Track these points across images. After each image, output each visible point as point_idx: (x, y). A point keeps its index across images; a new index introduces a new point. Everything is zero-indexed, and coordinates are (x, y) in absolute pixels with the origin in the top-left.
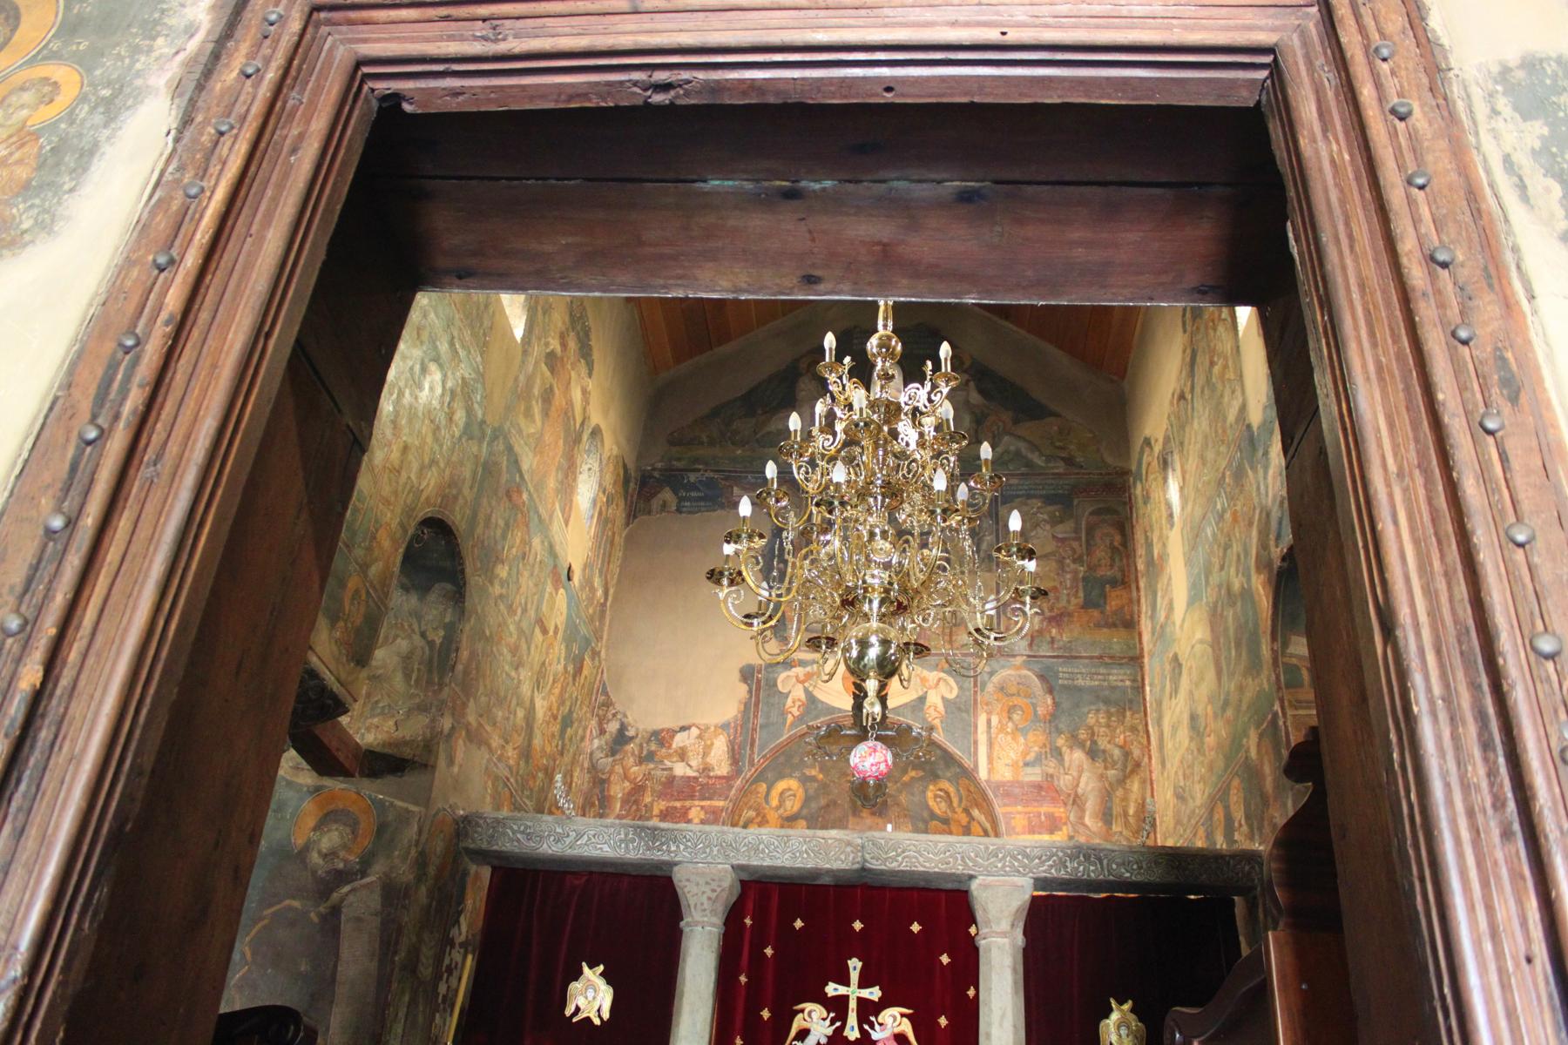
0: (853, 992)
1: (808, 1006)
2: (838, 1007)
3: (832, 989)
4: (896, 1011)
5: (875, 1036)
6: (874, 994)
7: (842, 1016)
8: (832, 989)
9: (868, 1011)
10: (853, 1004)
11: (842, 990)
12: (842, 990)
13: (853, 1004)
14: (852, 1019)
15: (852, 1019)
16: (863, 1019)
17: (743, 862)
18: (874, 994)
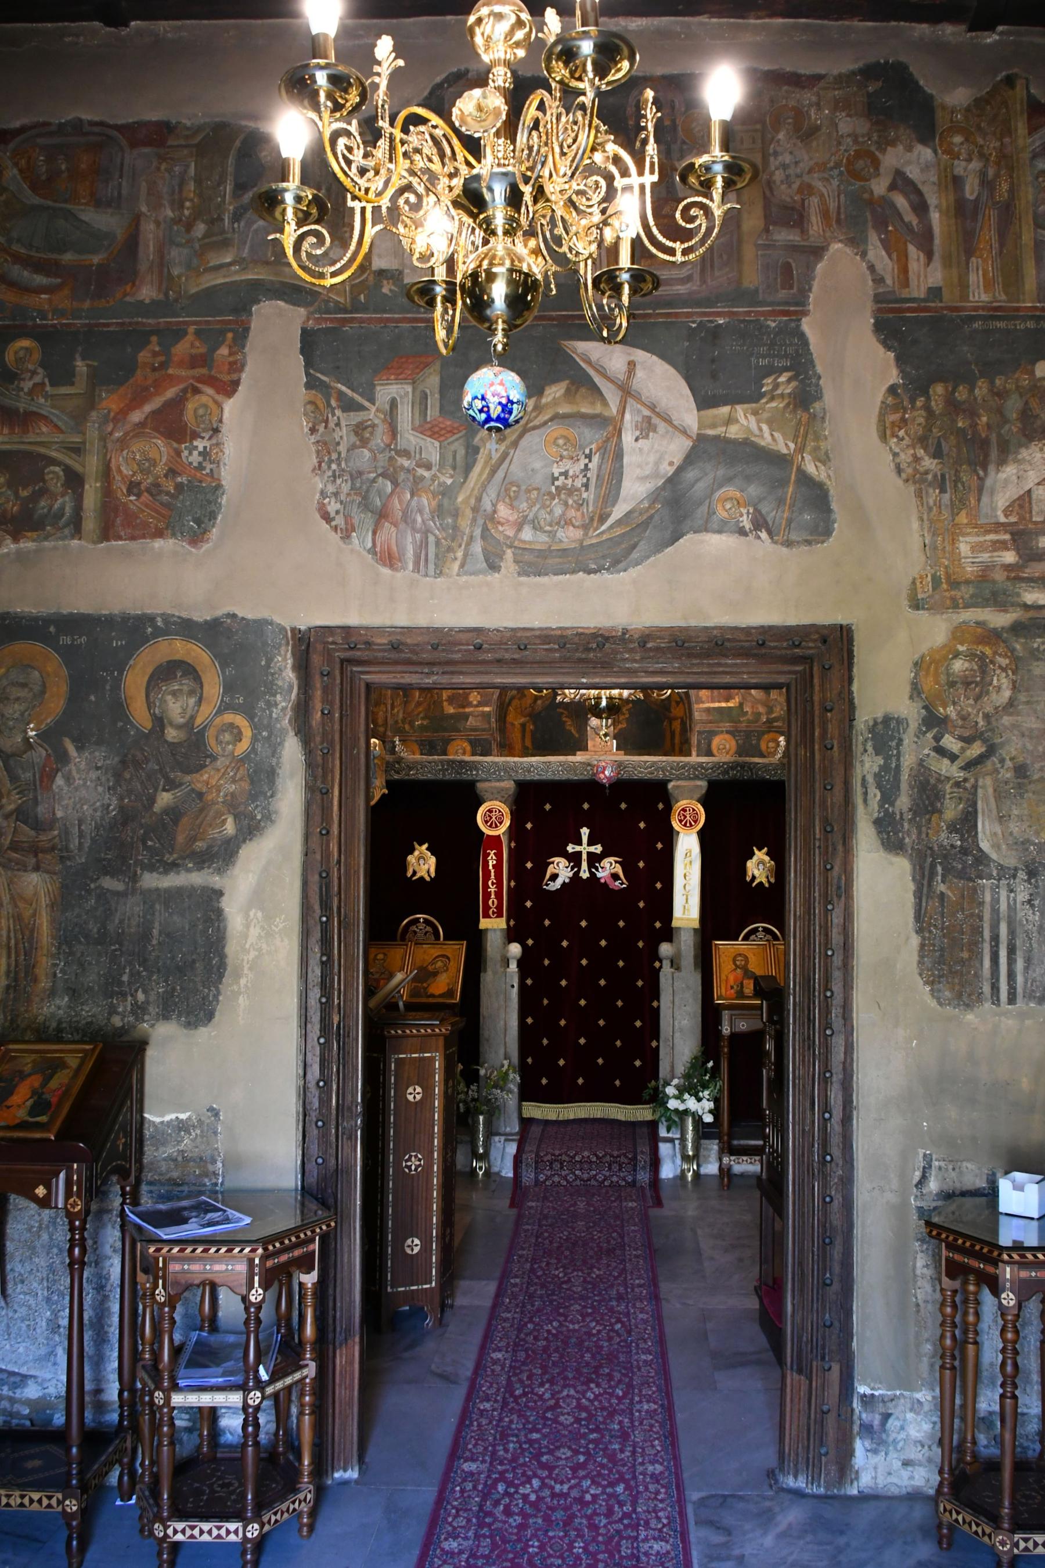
0: (584, 849)
1: (557, 859)
2: (575, 859)
3: (571, 848)
4: (612, 859)
5: (599, 875)
6: (598, 849)
7: (578, 865)
8: (571, 848)
9: (594, 860)
10: (584, 856)
11: (578, 848)
12: (578, 848)
13: (584, 856)
14: (584, 865)
15: (584, 865)
16: (591, 865)
17: (521, 778)
18: (598, 849)
